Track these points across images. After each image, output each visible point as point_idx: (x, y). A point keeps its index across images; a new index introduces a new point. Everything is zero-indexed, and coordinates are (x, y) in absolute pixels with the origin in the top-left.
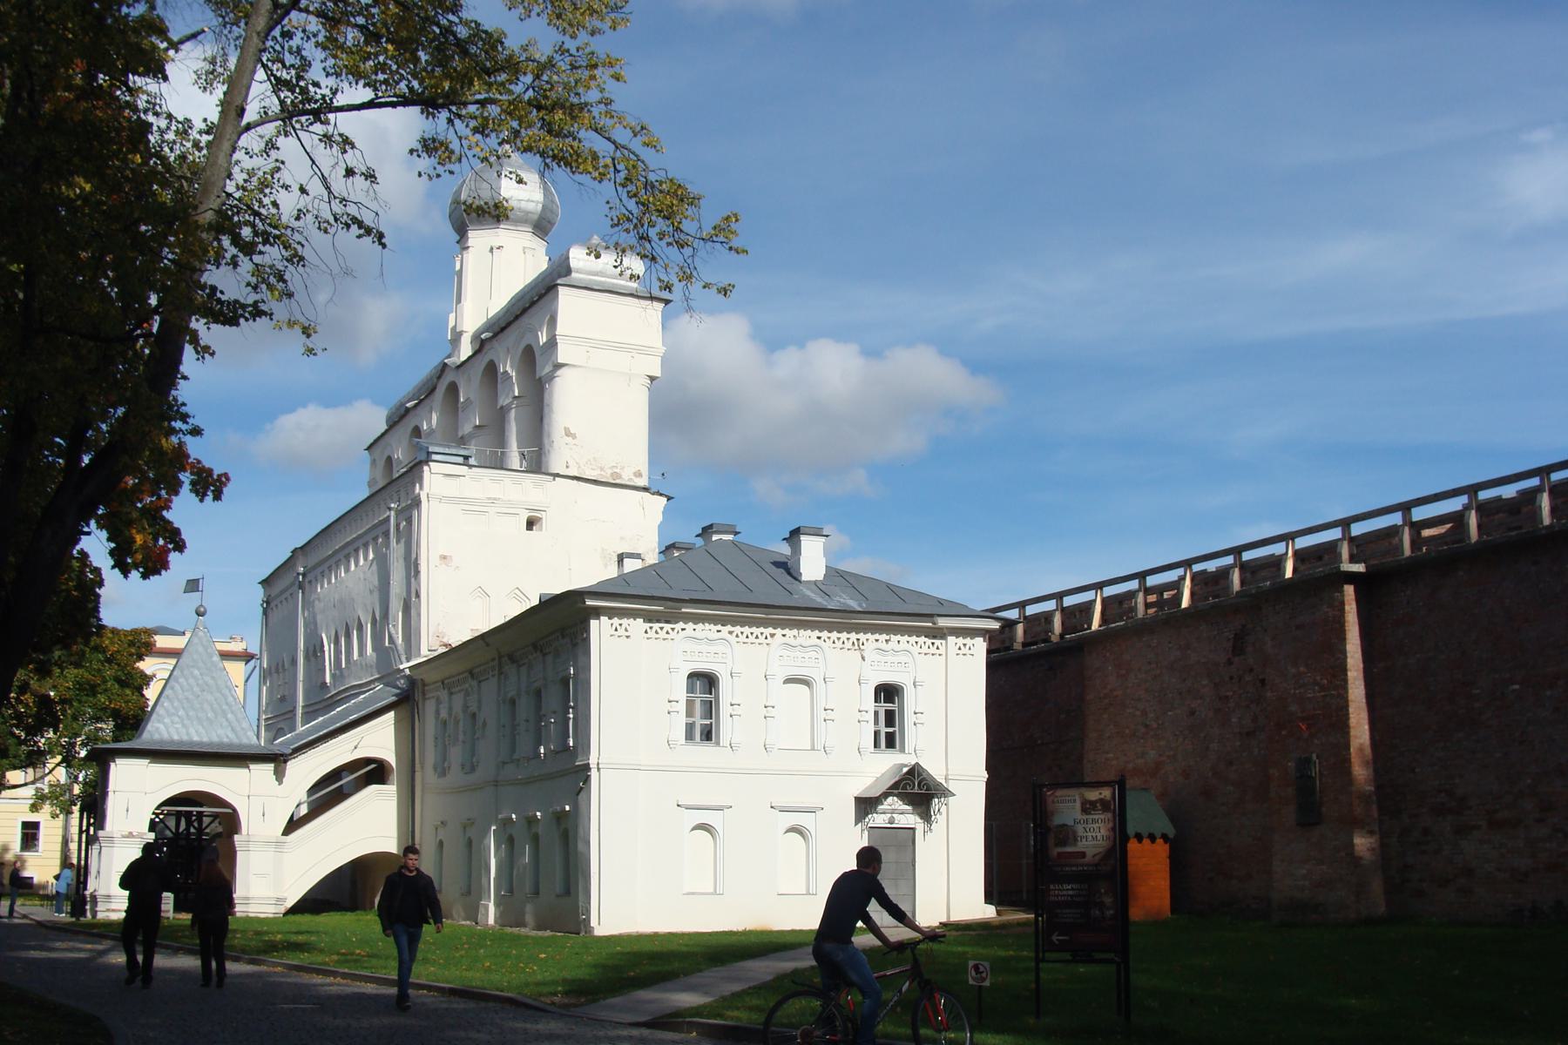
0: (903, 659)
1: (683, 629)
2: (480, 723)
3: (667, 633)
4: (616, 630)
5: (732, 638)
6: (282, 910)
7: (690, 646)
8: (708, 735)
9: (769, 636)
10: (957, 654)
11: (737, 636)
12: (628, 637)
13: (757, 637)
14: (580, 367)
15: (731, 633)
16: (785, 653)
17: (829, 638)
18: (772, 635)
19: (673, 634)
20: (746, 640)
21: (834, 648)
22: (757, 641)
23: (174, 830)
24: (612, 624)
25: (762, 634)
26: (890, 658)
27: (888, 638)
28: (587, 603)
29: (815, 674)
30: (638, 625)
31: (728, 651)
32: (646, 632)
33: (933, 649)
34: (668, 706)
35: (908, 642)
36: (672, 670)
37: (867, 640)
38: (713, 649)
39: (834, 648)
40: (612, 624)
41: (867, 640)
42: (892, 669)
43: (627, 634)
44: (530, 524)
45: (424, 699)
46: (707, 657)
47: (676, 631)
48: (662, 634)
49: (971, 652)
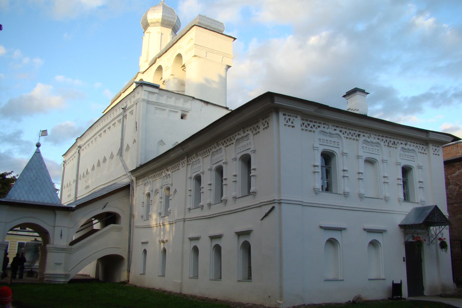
0: (411, 154)
1: (319, 127)
3: (311, 127)
6: (68, 280)
7: (322, 137)
8: (328, 188)
9: (357, 136)
10: (434, 154)
11: (343, 134)
13: (352, 135)
14: (202, 58)
15: (341, 131)
16: (365, 145)
18: (359, 135)
19: (314, 129)
22: (352, 137)
24: (285, 118)
25: (354, 134)
26: (407, 153)
27: (406, 143)
28: (276, 102)
30: (298, 121)
31: (340, 141)
33: (423, 151)
34: (313, 169)
35: (413, 146)
36: (315, 148)
38: (333, 139)
41: (398, 143)
42: (408, 159)
47: (315, 127)
48: (309, 128)
49: (438, 153)
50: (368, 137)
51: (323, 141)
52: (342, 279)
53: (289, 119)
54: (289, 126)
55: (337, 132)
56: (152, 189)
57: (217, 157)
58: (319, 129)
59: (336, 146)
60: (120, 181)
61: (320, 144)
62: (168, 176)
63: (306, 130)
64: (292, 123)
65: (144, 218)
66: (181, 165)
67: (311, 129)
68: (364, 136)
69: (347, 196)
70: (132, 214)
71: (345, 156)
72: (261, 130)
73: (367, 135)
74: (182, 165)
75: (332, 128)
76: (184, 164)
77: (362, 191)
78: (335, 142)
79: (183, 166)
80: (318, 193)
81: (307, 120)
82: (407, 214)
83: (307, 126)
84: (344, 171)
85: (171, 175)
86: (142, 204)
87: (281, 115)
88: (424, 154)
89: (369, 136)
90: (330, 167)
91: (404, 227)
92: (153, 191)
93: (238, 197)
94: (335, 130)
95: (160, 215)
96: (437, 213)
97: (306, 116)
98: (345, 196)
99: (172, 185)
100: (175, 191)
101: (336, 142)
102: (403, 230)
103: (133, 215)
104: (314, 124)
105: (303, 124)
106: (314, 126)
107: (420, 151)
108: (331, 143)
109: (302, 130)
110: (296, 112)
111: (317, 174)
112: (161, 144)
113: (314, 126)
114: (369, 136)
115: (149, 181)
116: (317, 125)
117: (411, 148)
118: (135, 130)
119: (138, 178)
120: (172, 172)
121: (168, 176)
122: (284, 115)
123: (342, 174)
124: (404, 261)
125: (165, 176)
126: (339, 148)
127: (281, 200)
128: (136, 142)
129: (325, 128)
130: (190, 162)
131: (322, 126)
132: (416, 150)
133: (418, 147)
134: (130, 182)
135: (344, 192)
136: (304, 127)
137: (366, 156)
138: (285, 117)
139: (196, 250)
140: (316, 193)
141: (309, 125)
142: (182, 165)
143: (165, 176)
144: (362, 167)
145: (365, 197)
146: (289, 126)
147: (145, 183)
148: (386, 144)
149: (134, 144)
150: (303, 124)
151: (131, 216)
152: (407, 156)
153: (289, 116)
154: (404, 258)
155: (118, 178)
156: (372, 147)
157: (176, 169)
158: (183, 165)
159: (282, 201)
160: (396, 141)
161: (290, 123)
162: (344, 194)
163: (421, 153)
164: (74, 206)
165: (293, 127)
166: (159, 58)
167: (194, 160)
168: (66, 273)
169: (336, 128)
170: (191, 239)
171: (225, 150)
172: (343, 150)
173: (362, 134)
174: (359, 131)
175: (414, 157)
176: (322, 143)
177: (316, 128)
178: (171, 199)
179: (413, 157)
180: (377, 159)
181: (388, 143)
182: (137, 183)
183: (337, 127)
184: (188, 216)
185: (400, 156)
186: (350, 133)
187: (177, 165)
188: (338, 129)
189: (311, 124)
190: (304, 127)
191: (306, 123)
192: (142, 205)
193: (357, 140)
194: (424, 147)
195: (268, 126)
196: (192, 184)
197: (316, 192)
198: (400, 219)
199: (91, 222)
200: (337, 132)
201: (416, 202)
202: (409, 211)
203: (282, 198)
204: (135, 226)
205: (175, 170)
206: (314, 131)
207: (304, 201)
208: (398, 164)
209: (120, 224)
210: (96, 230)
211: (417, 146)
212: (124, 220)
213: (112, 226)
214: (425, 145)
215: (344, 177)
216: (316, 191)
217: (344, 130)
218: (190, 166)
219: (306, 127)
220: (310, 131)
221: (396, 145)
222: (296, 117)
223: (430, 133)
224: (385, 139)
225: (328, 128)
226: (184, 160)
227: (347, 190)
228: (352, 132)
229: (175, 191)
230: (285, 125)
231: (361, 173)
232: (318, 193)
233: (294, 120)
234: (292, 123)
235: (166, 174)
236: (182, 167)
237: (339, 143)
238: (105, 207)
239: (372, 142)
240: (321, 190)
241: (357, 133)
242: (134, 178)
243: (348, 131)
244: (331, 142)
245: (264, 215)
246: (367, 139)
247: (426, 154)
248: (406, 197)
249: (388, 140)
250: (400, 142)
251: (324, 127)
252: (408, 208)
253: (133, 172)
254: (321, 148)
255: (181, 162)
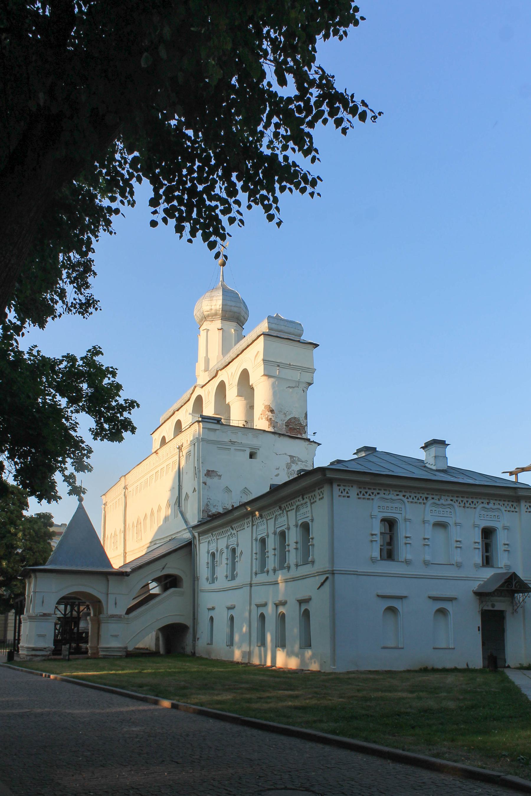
0: (496, 514)
1: (378, 493)
2: (238, 553)
3: (370, 495)
4: (342, 493)
5: (405, 499)
9: (425, 499)
11: (407, 498)
12: (348, 497)
13: (418, 499)
15: (404, 496)
16: (434, 509)
17: (457, 501)
18: (427, 498)
19: (373, 496)
20: (412, 501)
21: (460, 506)
22: (419, 501)
23: (63, 613)
24: (339, 489)
25: (421, 497)
26: (489, 513)
27: (488, 501)
28: (327, 476)
29: (451, 521)
30: (354, 491)
31: (403, 507)
32: (358, 495)
33: (513, 509)
34: (370, 538)
35: (499, 504)
36: (372, 517)
37: (478, 502)
38: (395, 505)
39: (460, 506)
40: (339, 489)
41: (478, 502)
42: (491, 519)
43: (348, 495)
44: (252, 456)
45: (199, 543)
46: (391, 509)
47: (374, 494)
48: (367, 496)
50: (438, 499)
51: (383, 508)
52: (402, 647)
53: (344, 490)
54: (344, 496)
55: (401, 497)
56: (217, 548)
57: (282, 520)
58: (378, 496)
59: (398, 512)
60: (180, 536)
61: (379, 512)
62: (234, 535)
63: (364, 498)
64: (347, 493)
65: (209, 580)
66: (246, 524)
67: (369, 497)
68: (433, 498)
69: (409, 564)
70: (196, 576)
71: (408, 523)
72: (317, 500)
73: (436, 497)
74: (247, 525)
75: (393, 494)
76: (249, 524)
77: (428, 558)
78: (397, 508)
79: (247, 526)
80: (375, 562)
81: (365, 488)
82: (486, 580)
83: (365, 494)
84: (406, 537)
85: (236, 534)
86: (207, 565)
87: (335, 487)
88: (514, 513)
89: (439, 498)
90: (393, 534)
91: (480, 595)
92: (218, 550)
93: (299, 565)
94: (398, 495)
95: (227, 578)
96: (514, 581)
97: (361, 485)
98: (407, 564)
99: (238, 545)
100: (241, 553)
101: (398, 508)
102: (478, 597)
103: (197, 577)
104: (373, 491)
105: (361, 492)
106: (373, 493)
107: (508, 509)
108: (393, 510)
109: (359, 498)
110: (351, 483)
111: (374, 543)
112: (226, 492)
113: (373, 493)
114: (439, 498)
115: (213, 539)
116: (375, 492)
117: (497, 506)
118: (194, 477)
119: (200, 534)
120: (238, 531)
121: (234, 535)
122: (338, 485)
123: (404, 541)
124: (479, 630)
125: (231, 535)
126: (401, 513)
127: (334, 570)
128: (196, 490)
129: (386, 494)
130: (255, 522)
131: (382, 492)
132: (503, 508)
133: (506, 505)
134: (191, 539)
135: (406, 560)
136: (361, 496)
137: (433, 520)
138: (339, 487)
139: (262, 617)
140: (373, 562)
141: (366, 493)
142: (247, 525)
143: (231, 535)
144: (429, 532)
145: (432, 564)
146: (344, 496)
147: (209, 541)
148: (462, 505)
149: (194, 493)
150: (361, 492)
151: (195, 579)
152: (489, 516)
153: (344, 486)
154: (479, 627)
155: (178, 532)
156: (444, 510)
157: (242, 528)
158: (248, 525)
159: (335, 572)
160: (475, 501)
161: (344, 494)
162: (406, 562)
163: (509, 511)
164: (129, 570)
165: (348, 497)
166: (221, 370)
167: (259, 521)
168: (125, 645)
169: (398, 493)
170: (258, 606)
171: (287, 515)
172: (405, 517)
173: (430, 497)
174: (427, 494)
175: (498, 517)
176: (381, 510)
177: (375, 495)
178: (237, 562)
179: (498, 516)
180: (449, 523)
181: (465, 504)
182: (199, 540)
183: (400, 491)
184: (255, 580)
185: (480, 517)
186: (416, 497)
187: (242, 524)
188: (401, 494)
189: (370, 492)
190: (361, 496)
191: (363, 491)
192: (207, 566)
193: (424, 503)
194: (515, 504)
195: (323, 497)
196: (257, 547)
197: (373, 561)
198: (475, 586)
199: (147, 586)
200: (401, 497)
201: (500, 567)
202: (488, 577)
203: (334, 569)
204: (200, 590)
205: (240, 529)
206: (372, 499)
207: (359, 571)
208: (475, 526)
209: (182, 588)
210: (155, 596)
211: (504, 504)
212: (186, 582)
213: (172, 590)
214: (516, 502)
215: (406, 544)
216: (373, 560)
217: (408, 495)
218: (255, 527)
219: (363, 495)
220: (368, 499)
221: (475, 505)
222: (352, 486)
223: (519, 489)
224: (460, 499)
225: (389, 494)
226: (249, 520)
227: (409, 557)
228: (418, 496)
229: (241, 553)
230: (340, 496)
231: (428, 539)
232: (375, 562)
233: (349, 490)
234: (347, 493)
235: (231, 533)
236: (247, 527)
237: (401, 508)
238: (163, 568)
239: (442, 504)
240: (379, 558)
241: (424, 496)
242: (196, 535)
243: (413, 495)
244: (392, 508)
245: (320, 584)
246: (437, 502)
247: (516, 512)
248: (488, 561)
249: (465, 500)
250: (480, 501)
251: (384, 494)
252: (488, 573)
253: (195, 527)
254: (381, 516)
255: (246, 521)
